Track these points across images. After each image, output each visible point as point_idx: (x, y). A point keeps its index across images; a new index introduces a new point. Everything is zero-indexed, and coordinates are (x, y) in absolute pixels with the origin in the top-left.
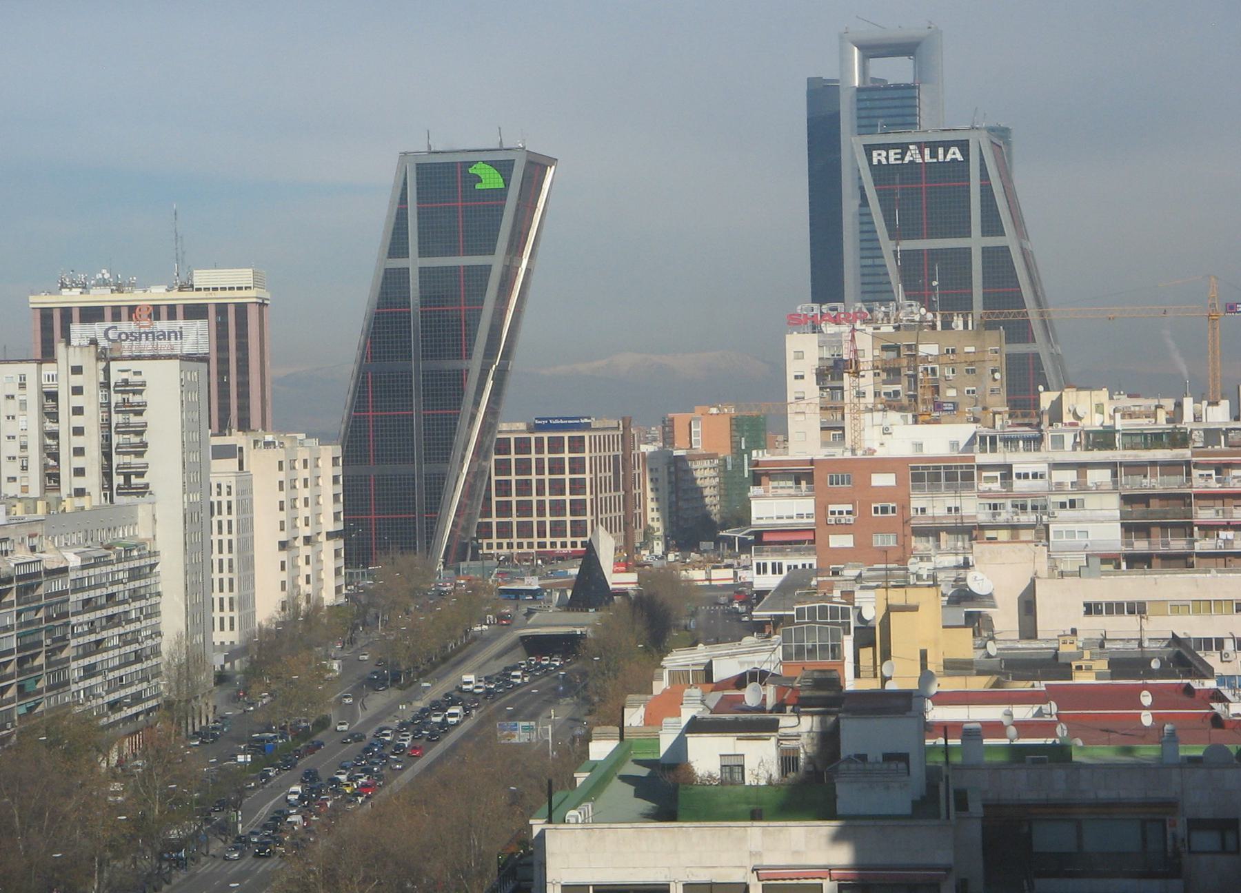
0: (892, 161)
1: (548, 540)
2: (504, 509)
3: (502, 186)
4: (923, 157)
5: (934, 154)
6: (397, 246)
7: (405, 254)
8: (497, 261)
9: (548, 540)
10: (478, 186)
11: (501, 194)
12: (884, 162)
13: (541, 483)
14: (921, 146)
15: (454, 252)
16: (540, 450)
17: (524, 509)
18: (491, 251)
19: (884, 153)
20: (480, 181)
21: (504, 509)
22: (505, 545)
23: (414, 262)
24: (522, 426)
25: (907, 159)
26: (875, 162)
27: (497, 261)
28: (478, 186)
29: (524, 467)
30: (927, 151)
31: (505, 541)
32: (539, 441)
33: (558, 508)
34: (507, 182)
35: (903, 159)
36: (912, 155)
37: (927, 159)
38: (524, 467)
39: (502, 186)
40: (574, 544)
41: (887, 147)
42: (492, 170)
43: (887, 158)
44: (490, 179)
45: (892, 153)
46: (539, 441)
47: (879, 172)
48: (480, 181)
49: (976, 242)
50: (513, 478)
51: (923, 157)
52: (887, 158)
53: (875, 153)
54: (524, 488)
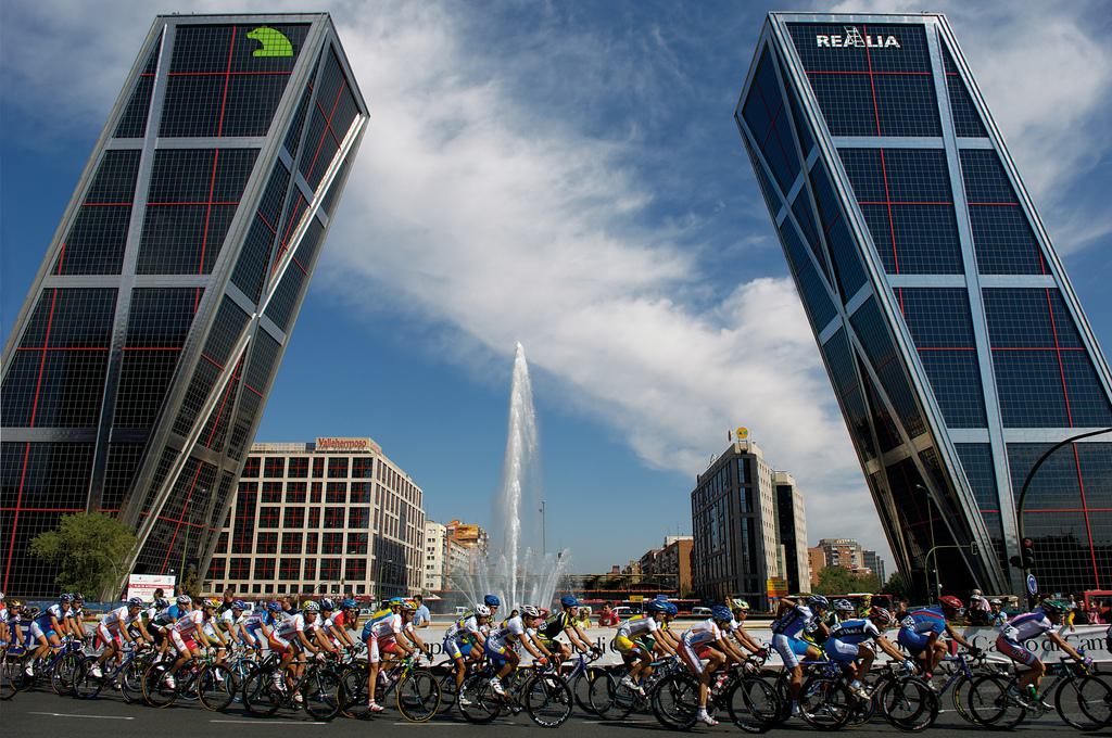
1: (317, 582)
2: (267, 543)
3: (289, 53)
4: (865, 40)
7: (140, 132)
8: (268, 145)
9: (317, 582)
10: (257, 53)
11: (283, 67)
13: (315, 512)
15: (212, 133)
16: (318, 473)
17: (292, 543)
18: (263, 132)
20: (260, 46)
21: (267, 543)
22: (263, 589)
23: (150, 143)
24: (303, 447)
27: (268, 145)
28: (257, 53)
29: (297, 492)
31: (263, 583)
32: (319, 462)
33: (332, 543)
34: (297, 50)
37: (869, 42)
38: (297, 492)
39: (289, 53)
40: (348, 589)
42: (279, 35)
44: (274, 45)
46: (319, 462)
48: (260, 46)
49: (951, 143)
50: (283, 505)
54: (295, 517)
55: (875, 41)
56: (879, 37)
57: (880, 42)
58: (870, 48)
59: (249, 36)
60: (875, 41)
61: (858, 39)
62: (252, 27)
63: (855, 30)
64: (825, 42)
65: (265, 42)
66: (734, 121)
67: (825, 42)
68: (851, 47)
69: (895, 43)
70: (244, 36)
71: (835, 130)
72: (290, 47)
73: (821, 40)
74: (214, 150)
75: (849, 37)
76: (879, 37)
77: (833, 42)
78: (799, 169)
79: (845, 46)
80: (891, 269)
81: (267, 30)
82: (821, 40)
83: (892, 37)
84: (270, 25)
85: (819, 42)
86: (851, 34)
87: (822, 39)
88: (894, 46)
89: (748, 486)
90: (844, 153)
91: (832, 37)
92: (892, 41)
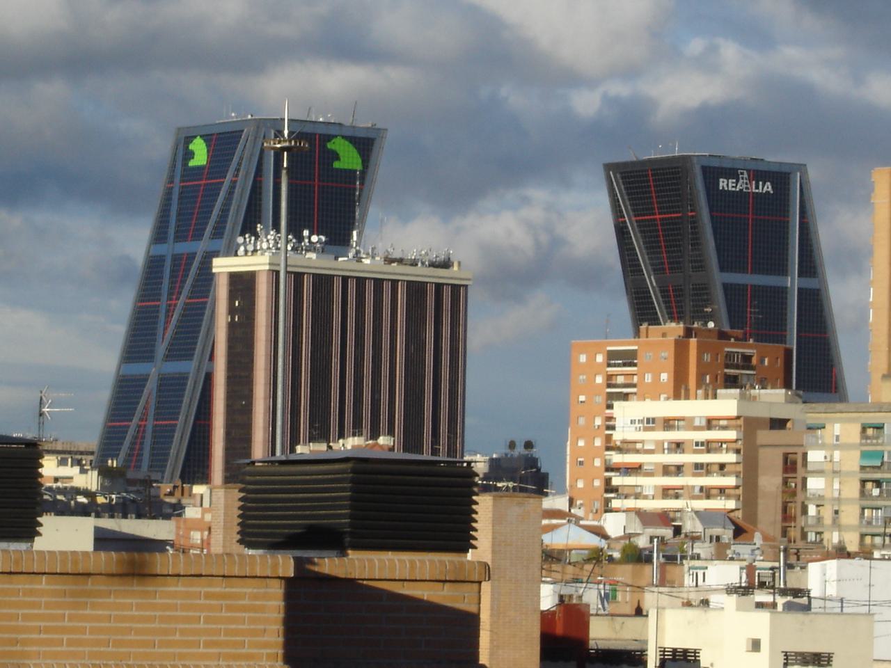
4: (751, 186)
10: (336, 165)
20: (336, 156)
28: (336, 165)
35: (736, 187)
49: (793, 282)
55: (757, 187)
56: (761, 183)
57: (761, 187)
58: (753, 193)
59: (330, 146)
60: (757, 187)
61: (746, 184)
62: (329, 138)
63: (746, 175)
64: (725, 186)
65: (341, 154)
67: (725, 186)
68: (741, 190)
69: (770, 189)
70: (325, 146)
71: (722, 269)
72: (360, 161)
73: (723, 183)
75: (741, 181)
76: (761, 183)
77: (730, 185)
79: (738, 190)
81: (342, 141)
82: (723, 183)
83: (769, 183)
84: (343, 137)
85: (721, 184)
86: (743, 178)
87: (723, 182)
88: (769, 192)
90: (727, 287)
91: (730, 181)
92: (768, 188)
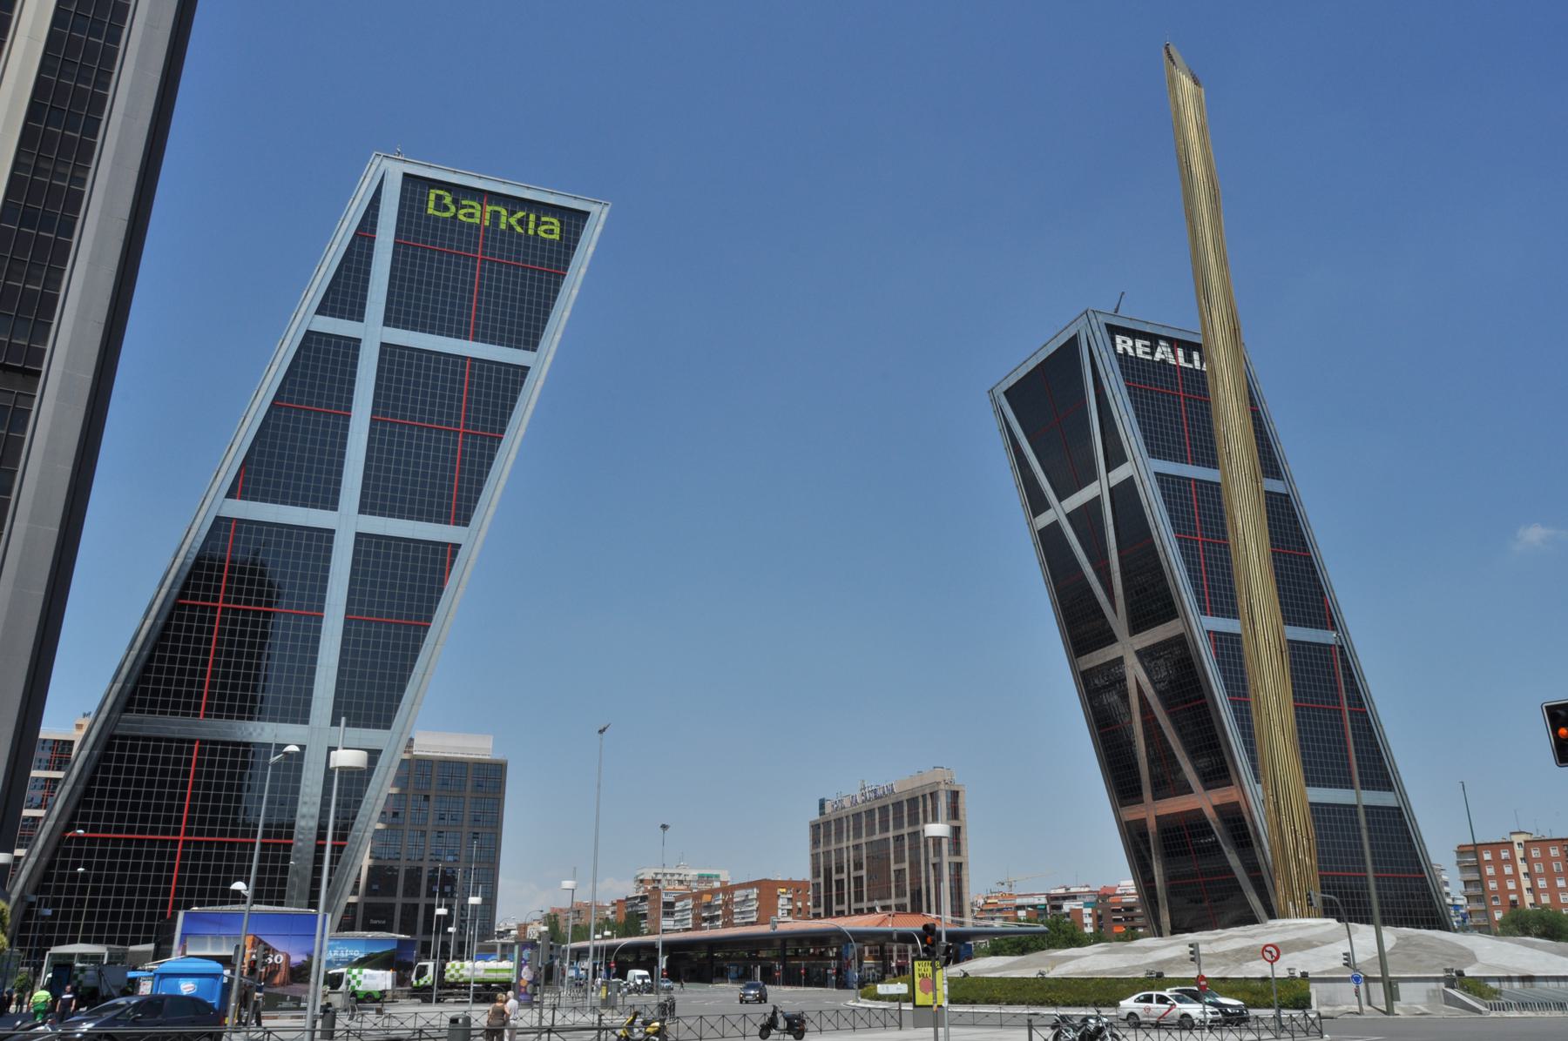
0: (1140, 353)
4: (1176, 358)
5: (1189, 359)
6: (345, 296)
7: (357, 313)
12: (1131, 352)
14: (1174, 343)
19: (1130, 342)
25: (1158, 356)
26: (1120, 349)
30: (1180, 352)
35: (1153, 354)
36: (1162, 352)
41: (1134, 334)
43: (1134, 348)
45: (1139, 343)
47: (1127, 363)
51: (1176, 358)
52: (1134, 348)
53: (1119, 339)
66: (987, 398)
68: (1164, 361)
74: (466, 358)
78: (1092, 476)
80: (1203, 610)
89: (956, 823)
